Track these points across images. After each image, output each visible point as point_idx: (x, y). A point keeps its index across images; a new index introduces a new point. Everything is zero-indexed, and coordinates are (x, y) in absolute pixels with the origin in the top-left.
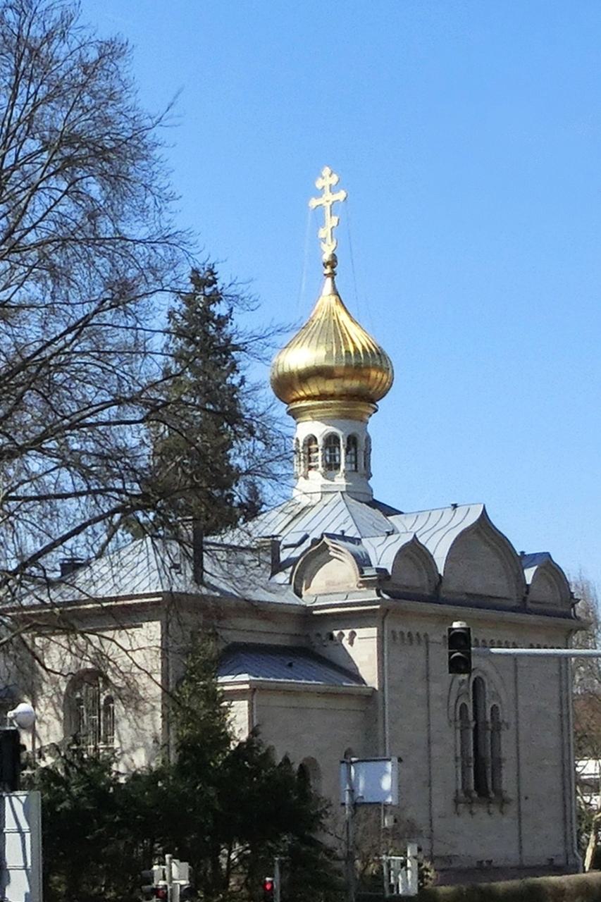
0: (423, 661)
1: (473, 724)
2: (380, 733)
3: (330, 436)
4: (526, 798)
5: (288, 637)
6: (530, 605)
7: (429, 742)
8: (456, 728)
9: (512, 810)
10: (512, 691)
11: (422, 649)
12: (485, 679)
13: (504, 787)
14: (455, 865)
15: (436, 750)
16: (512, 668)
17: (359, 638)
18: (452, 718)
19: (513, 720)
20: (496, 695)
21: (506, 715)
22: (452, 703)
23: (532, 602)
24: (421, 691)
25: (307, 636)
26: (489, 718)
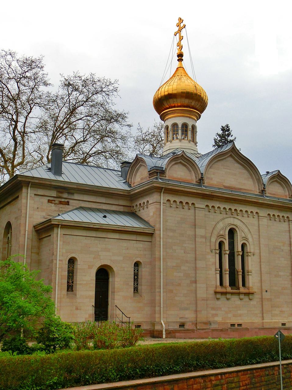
0: (193, 218)
1: (228, 252)
2: (157, 253)
3: (175, 124)
4: (266, 291)
5: (122, 207)
6: (267, 195)
7: (196, 260)
8: (216, 253)
9: (257, 297)
10: (256, 236)
11: (192, 211)
12: (237, 229)
13: (251, 285)
14: (213, 326)
15: (200, 264)
16: (257, 225)
17: (150, 204)
18: (213, 248)
19: (257, 251)
20: (246, 238)
21: (250, 248)
22: (213, 240)
23: (268, 193)
24: (190, 232)
25: (133, 207)
26: (240, 249)
